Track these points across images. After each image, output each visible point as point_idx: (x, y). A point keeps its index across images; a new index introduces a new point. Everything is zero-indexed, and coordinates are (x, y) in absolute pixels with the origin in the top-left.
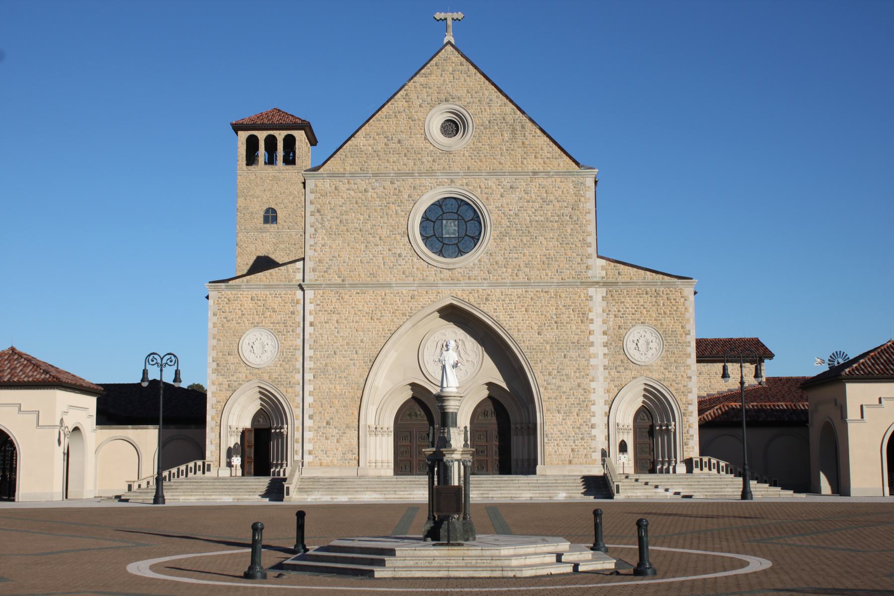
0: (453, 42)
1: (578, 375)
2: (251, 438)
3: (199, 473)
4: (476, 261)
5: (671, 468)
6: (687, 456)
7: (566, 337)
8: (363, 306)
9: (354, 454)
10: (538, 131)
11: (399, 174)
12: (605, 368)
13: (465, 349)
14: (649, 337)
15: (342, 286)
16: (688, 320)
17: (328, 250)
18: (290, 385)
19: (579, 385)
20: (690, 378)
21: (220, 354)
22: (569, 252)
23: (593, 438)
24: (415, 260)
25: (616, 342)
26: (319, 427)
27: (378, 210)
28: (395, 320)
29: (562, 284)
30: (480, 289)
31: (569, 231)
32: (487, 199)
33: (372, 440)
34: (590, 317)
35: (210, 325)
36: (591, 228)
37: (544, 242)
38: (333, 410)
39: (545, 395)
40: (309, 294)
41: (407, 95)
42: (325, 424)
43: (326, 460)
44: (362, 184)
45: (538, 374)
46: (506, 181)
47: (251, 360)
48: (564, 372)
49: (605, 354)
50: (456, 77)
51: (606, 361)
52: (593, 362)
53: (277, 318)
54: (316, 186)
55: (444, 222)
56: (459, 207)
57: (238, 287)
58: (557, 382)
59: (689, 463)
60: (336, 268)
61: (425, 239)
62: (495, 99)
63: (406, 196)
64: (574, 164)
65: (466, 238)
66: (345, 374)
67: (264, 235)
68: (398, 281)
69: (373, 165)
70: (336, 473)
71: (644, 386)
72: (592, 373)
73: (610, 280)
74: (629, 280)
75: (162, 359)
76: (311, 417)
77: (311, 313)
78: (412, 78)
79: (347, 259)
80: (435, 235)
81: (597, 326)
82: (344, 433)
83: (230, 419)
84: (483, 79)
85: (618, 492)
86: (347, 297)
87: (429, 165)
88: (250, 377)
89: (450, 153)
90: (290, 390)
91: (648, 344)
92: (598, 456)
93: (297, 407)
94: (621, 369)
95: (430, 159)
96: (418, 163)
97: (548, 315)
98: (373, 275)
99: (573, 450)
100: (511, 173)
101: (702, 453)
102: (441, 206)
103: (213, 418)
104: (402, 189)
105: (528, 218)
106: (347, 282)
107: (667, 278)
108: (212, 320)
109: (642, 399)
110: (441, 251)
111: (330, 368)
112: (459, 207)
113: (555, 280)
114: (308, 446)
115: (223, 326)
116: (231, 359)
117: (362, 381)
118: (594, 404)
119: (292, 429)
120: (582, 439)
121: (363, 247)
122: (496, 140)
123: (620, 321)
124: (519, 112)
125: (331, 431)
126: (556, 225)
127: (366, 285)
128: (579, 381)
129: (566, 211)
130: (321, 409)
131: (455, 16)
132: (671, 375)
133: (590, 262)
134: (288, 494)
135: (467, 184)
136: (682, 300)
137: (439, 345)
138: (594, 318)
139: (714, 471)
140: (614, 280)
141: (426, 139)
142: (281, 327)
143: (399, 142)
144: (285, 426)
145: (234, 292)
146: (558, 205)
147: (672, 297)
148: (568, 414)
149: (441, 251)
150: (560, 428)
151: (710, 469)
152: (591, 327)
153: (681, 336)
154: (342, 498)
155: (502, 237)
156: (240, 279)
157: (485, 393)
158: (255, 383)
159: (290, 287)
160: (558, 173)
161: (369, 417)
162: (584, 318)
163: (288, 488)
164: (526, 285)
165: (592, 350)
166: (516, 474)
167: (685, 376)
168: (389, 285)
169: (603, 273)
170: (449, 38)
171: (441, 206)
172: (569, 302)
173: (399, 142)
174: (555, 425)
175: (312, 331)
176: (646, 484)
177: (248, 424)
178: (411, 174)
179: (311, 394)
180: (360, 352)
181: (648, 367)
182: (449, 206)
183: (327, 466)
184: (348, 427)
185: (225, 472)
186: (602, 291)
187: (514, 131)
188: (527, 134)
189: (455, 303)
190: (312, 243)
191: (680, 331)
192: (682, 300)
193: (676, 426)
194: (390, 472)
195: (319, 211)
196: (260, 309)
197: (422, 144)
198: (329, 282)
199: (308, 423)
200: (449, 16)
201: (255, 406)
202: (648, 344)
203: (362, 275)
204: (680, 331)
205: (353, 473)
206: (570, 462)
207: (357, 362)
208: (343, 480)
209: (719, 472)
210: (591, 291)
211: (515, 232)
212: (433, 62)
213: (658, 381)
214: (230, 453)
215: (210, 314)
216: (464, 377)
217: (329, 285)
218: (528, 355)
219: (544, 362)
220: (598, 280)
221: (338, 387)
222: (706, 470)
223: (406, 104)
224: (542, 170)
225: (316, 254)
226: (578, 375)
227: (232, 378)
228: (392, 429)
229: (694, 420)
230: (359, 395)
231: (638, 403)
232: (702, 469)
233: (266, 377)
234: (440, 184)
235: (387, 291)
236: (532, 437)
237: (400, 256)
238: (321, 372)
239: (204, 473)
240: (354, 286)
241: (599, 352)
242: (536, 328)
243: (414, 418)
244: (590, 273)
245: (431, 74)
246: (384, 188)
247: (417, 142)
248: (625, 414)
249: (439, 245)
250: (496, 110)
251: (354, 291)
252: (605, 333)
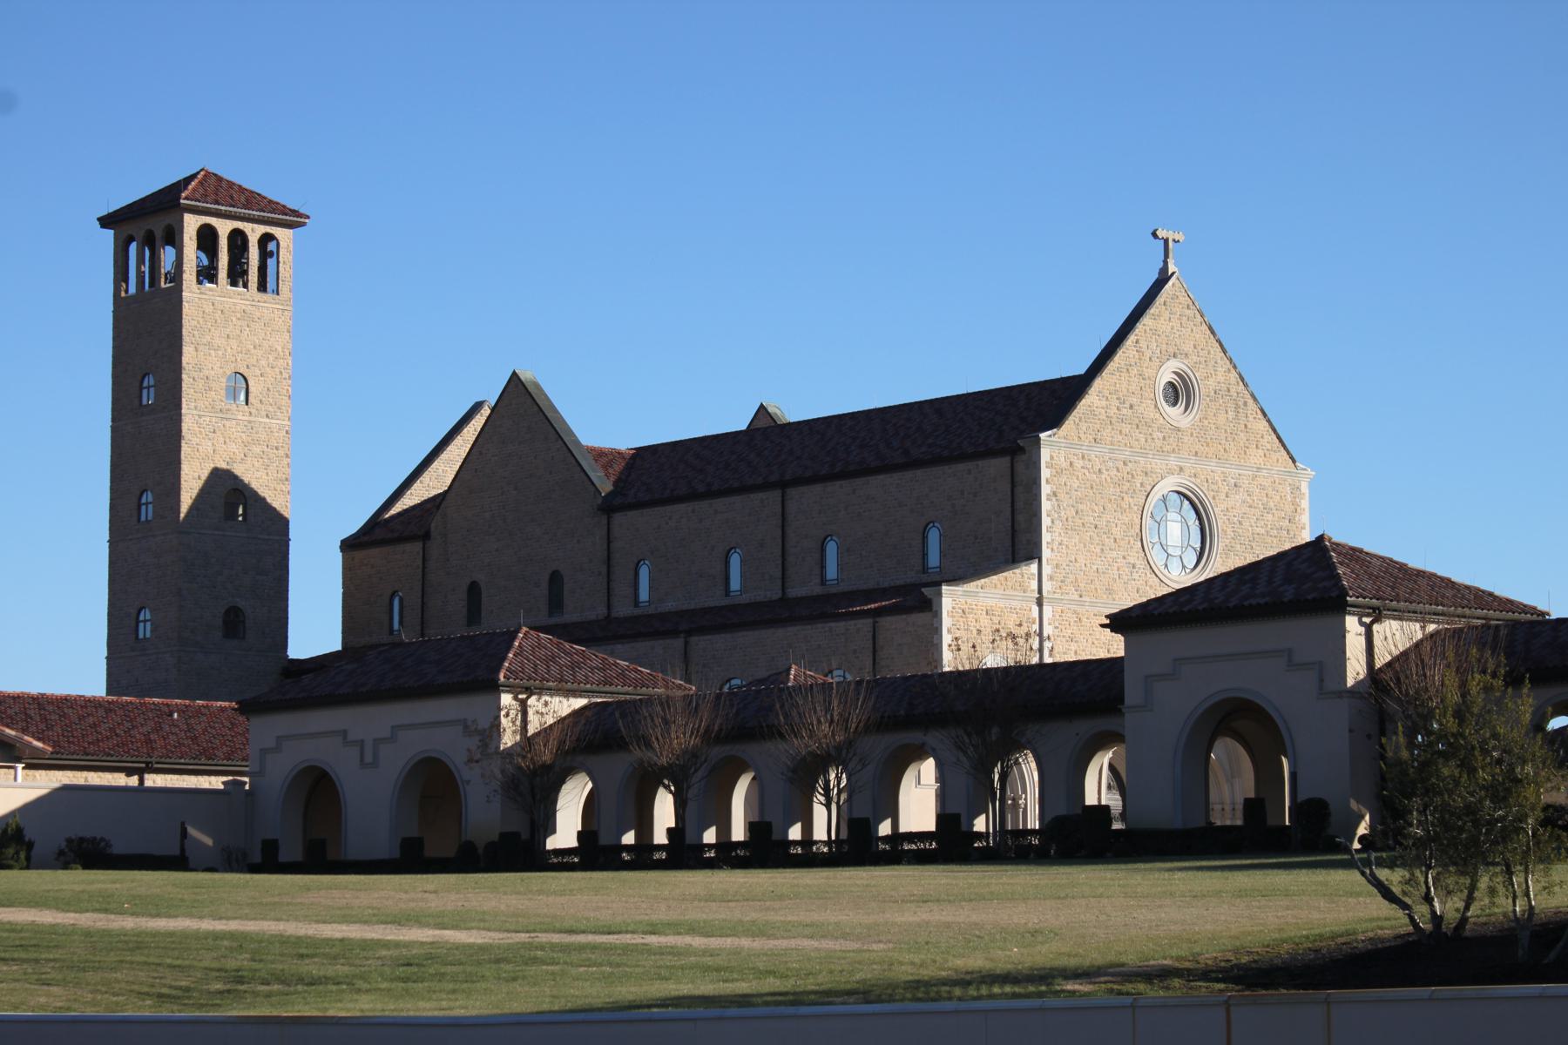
40: (1047, 610)
67: (228, 424)
122: (1222, 418)
187: (1237, 407)
197: (1151, 414)
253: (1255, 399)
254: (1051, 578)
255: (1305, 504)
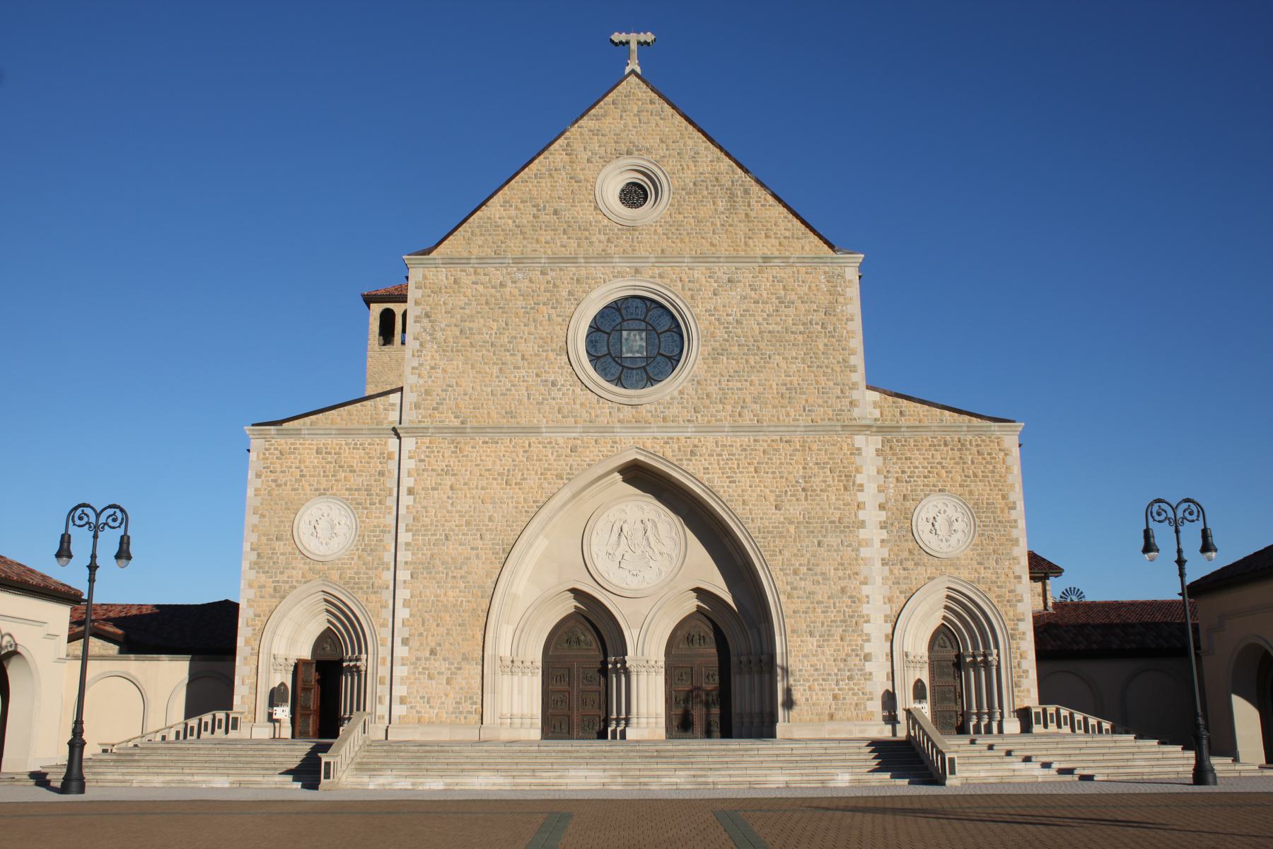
0: (638, 70)
1: (840, 573)
2: (313, 676)
3: (220, 733)
4: (676, 393)
5: (995, 725)
6: (1020, 704)
7: (821, 513)
8: (494, 462)
9: (475, 703)
10: (770, 198)
11: (554, 259)
12: (884, 562)
13: (657, 535)
14: (951, 512)
15: (460, 431)
16: (1012, 486)
17: (440, 375)
18: (375, 590)
19: (843, 590)
20: (1019, 577)
21: (264, 539)
22: (822, 379)
23: (868, 676)
24: (578, 390)
25: (900, 522)
26: (418, 659)
27: (521, 314)
28: (545, 485)
29: (813, 427)
30: (682, 436)
31: (821, 347)
32: (692, 297)
33: (505, 681)
34: (858, 481)
35: (250, 492)
36: (857, 343)
37: (783, 364)
38: (442, 630)
39: (788, 607)
40: (409, 443)
41: (568, 145)
42: (428, 654)
43: (428, 713)
44: (497, 275)
45: (776, 573)
46: (722, 270)
47: (312, 548)
48: (818, 570)
49: (883, 541)
50: (644, 119)
51: (885, 553)
52: (864, 552)
53: (356, 481)
54: (425, 277)
55: (625, 333)
56: (648, 310)
57: (297, 433)
58: (807, 585)
59: (1025, 716)
60: (452, 403)
61: (594, 359)
62: (703, 152)
63: (565, 294)
64: (826, 247)
65: (659, 358)
66: (462, 572)
68: (551, 424)
69: (515, 246)
70: (444, 735)
71: (946, 592)
72: (864, 571)
73: (887, 423)
74: (917, 423)
75: (98, 515)
76: (405, 642)
77: (409, 475)
78: (577, 121)
79: (470, 391)
80: (609, 354)
81: (870, 496)
82: (460, 669)
83: (274, 647)
84: (685, 123)
85: (953, 772)
86: (468, 448)
87: (601, 246)
88: (310, 575)
89: (634, 228)
90: (373, 597)
91: (951, 524)
92: (876, 706)
93: (383, 625)
94: (910, 564)
95: (602, 237)
96: (585, 243)
97: (791, 477)
98: (511, 414)
99: (835, 697)
100: (730, 259)
101: (1043, 699)
102: (619, 310)
103: (247, 642)
104: (558, 282)
105: (756, 327)
106: (469, 425)
107: (975, 421)
108: (253, 483)
109: (942, 612)
110: (619, 378)
111: (438, 562)
112: (648, 310)
113: (802, 423)
114: (399, 691)
115: (270, 494)
116: (280, 546)
117: (490, 583)
118: (868, 621)
119: (374, 662)
120: (850, 678)
121: (495, 370)
123: (905, 488)
124: (739, 171)
125: (439, 665)
126: (800, 337)
127: (498, 429)
128: (843, 583)
129: (816, 317)
130: (422, 630)
131: (643, 37)
132: (988, 574)
133: (855, 395)
134: (327, 776)
135: (661, 276)
136: (1001, 455)
137: (616, 529)
138: (864, 482)
139: (1066, 729)
140: (894, 424)
141: (596, 208)
142: (361, 497)
143: (556, 212)
144: (364, 656)
145: (290, 441)
146: (803, 308)
147: (985, 450)
148: (826, 637)
149: (619, 378)
150: (814, 660)
151: (1059, 726)
152: (861, 497)
153: (1002, 511)
154: (433, 785)
155: (715, 355)
156: (301, 421)
157: (691, 604)
158: (317, 585)
159: (377, 432)
160: (801, 259)
161: (502, 641)
162: (848, 481)
163: (328, 764)
164: (757, 427)
165: (862, 534)
166: (741, 737)
167: (1011, 575)
168: (536, 430)
169: (877, 413)
170: (633, 65)
171: (619, 310)
172: (824, 457)
173: (556, 212)
174: (804, 656)
175: (411, 503)
176: (1009, 753)
177: (306, 653)
178: (572, 260)
179: (406, 603)
180: (488, 536)
181: (953, 563)
182: (632, 310)
183: (431, 723)
184: (465, 658)
185: (263, 732)
186: (876, 441)
187: (732, 197)
188: (753, 202)
189: (642, 458)
190: (416, 365)
191: (1000, 503)
192: (1001, 455)
193: (1001, 655)
194: (536, 734)
195: (427, 315)
196: (331, 467)
197: (590, 215)
198: (441, 425)
199: (400, 651)
200: (634, 38)
201: (318, 625)
202: (951, 524)
203: (494, 415)
204: (1000, 503)
205: (472, 735)
206: (831, 717)
207: (482, 553)
208: (440, 748)
209: (1073, 730)
210: (859, 440)
211: (736, 348)
212: (609, 99)
213: (971, 583)
214: (275, 697)
215: (251, 474)
216: (655, 582)
217: (440, 430)
218: (760, 542)
219: (787, 554)
220: (868, 422)
221: (450, 593)
222: (1052, 727)
223: (566, 158)
224: (776, 254)
225: (421, 381)
226: (840, 573)
227: (279, 577)
228: (540, 664)
229: (1028, 645)
230: (485, 607)
231: (936, 621)
232: (1046, 726)
233: (335, 575)
234: (619, 275)
235: (533, 439)
236: (767, 677)
237: (554, 384)
238: (422, 569)
239: (227, 732)
240: (480, 430)
241: (873, 534)
242: (772, 498)
243: (575, 646)
244: (856, 412)
245: (605, 115)
246: (531, 281)
247: (584, 213)
248: (916, 640)
249: (616, 370)
250: (704, 167)
251: (479, 439)
252: (882, 507)
253: (762, 185)
254: (417, 406)
255: (854, 291)
